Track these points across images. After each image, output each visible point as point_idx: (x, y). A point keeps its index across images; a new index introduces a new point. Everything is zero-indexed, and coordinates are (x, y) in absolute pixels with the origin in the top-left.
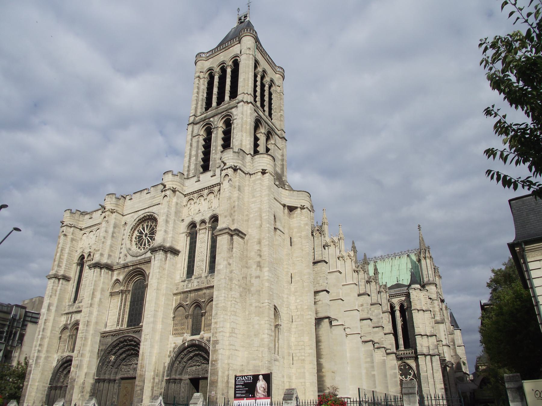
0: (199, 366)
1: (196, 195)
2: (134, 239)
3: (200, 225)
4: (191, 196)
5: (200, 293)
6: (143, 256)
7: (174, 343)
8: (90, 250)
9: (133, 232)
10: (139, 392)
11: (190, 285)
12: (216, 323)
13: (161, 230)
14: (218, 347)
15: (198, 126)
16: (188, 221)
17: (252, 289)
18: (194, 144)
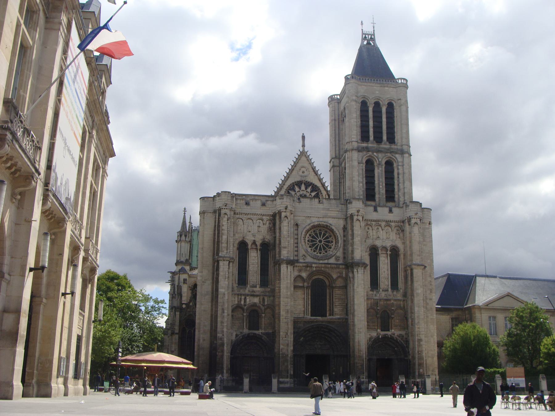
1: (374, 223)
2: (306, 241)
3: (381, 250)
4: (369, 222)
5: (388, 302)
6: (326, 261)
8: (253, 239)
10: (360, 367)
11: (378, 295)
12: (419, 328)
13: (358, 249)
14: (421, 343)
15: (361, 153)
16: (370, 242)
17: (428, 307)
18: (361, 172)
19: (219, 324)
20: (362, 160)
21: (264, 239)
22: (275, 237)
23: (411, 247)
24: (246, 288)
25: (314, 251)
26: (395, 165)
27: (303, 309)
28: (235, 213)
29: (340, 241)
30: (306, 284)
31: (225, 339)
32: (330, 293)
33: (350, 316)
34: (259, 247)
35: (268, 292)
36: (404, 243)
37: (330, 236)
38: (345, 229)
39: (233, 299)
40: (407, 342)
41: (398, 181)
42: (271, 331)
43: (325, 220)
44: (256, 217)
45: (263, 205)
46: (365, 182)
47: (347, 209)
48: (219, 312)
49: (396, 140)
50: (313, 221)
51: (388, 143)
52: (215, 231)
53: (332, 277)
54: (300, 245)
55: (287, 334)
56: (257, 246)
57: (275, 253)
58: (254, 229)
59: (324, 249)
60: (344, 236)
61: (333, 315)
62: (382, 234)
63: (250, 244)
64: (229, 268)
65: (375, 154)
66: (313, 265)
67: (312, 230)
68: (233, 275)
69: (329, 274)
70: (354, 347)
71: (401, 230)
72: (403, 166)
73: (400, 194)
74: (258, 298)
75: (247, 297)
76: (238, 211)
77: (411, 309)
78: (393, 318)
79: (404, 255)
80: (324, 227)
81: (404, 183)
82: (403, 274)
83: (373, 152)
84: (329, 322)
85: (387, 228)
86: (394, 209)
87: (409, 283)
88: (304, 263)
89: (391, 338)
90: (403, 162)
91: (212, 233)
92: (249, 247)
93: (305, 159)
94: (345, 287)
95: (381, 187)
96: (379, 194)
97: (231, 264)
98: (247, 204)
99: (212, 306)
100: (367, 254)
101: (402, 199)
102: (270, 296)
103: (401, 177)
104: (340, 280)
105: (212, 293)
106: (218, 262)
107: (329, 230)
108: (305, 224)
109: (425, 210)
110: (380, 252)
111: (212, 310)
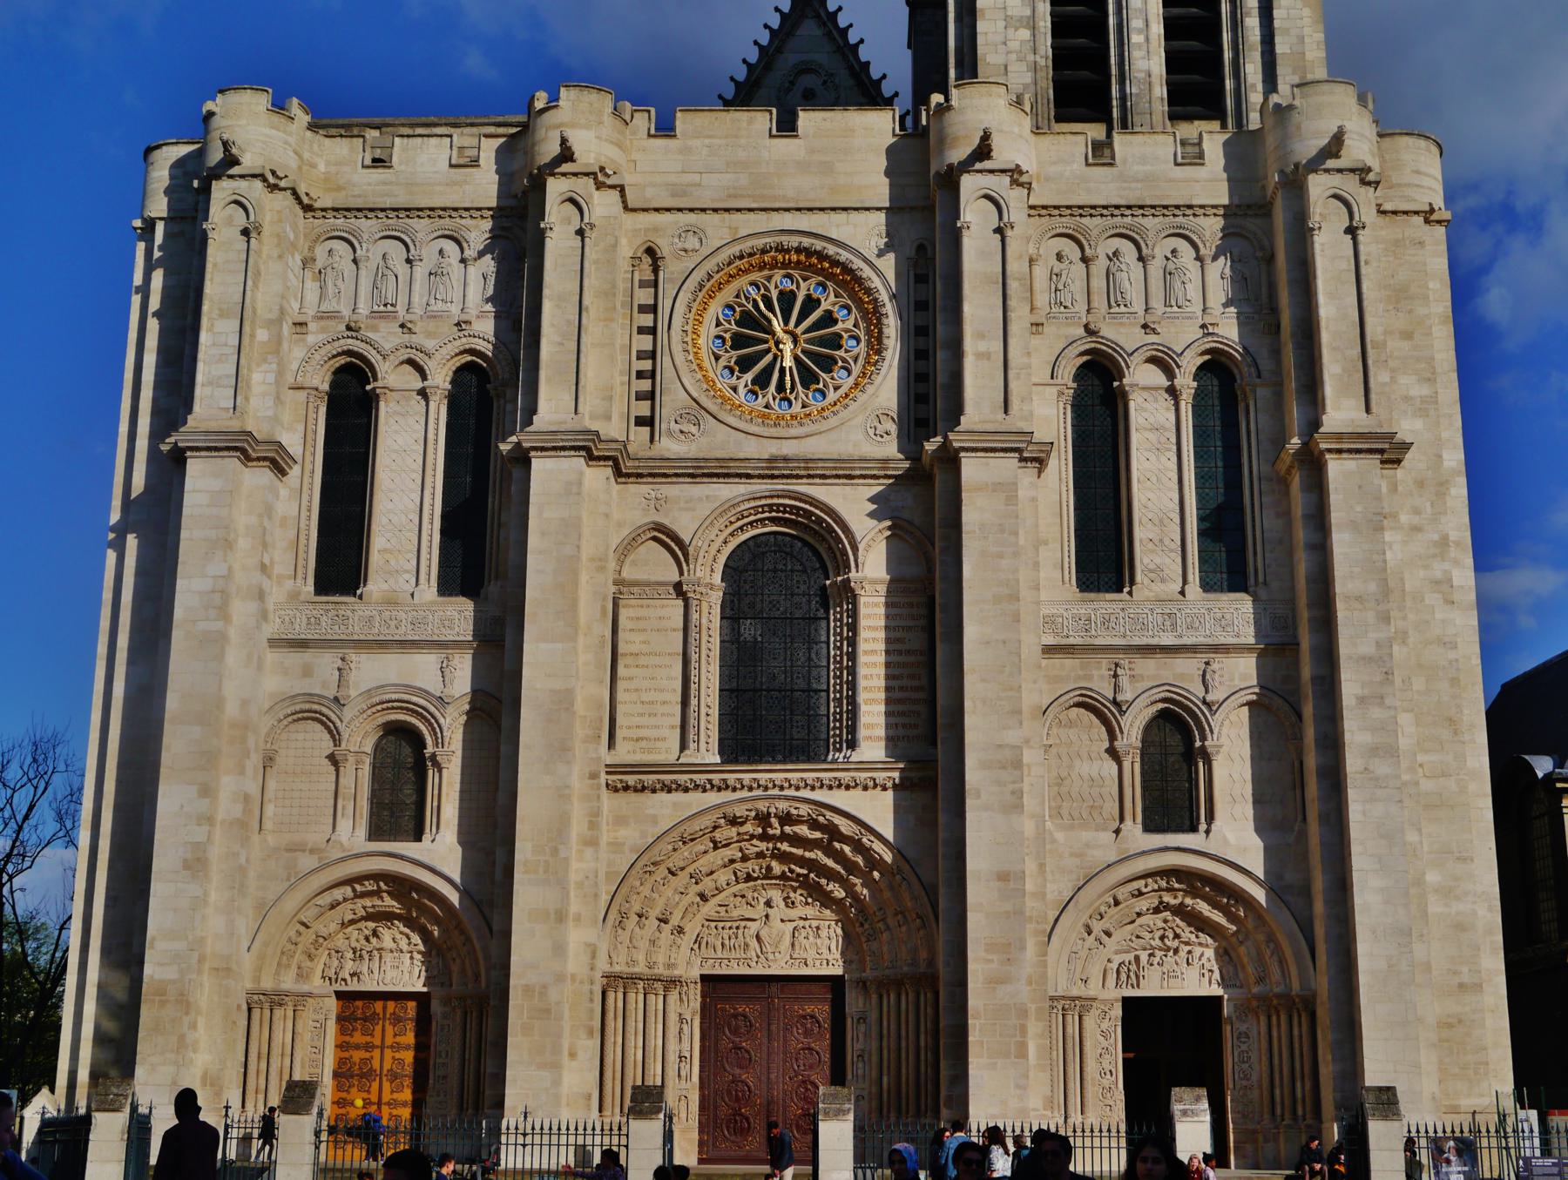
46: (1045, 24)
54: (665, 362)
59: (808, 379)
67: (742, 282)
93: (818, 32)
95: (1136, 38)
101: (1255, 97)
106: (178, 458)
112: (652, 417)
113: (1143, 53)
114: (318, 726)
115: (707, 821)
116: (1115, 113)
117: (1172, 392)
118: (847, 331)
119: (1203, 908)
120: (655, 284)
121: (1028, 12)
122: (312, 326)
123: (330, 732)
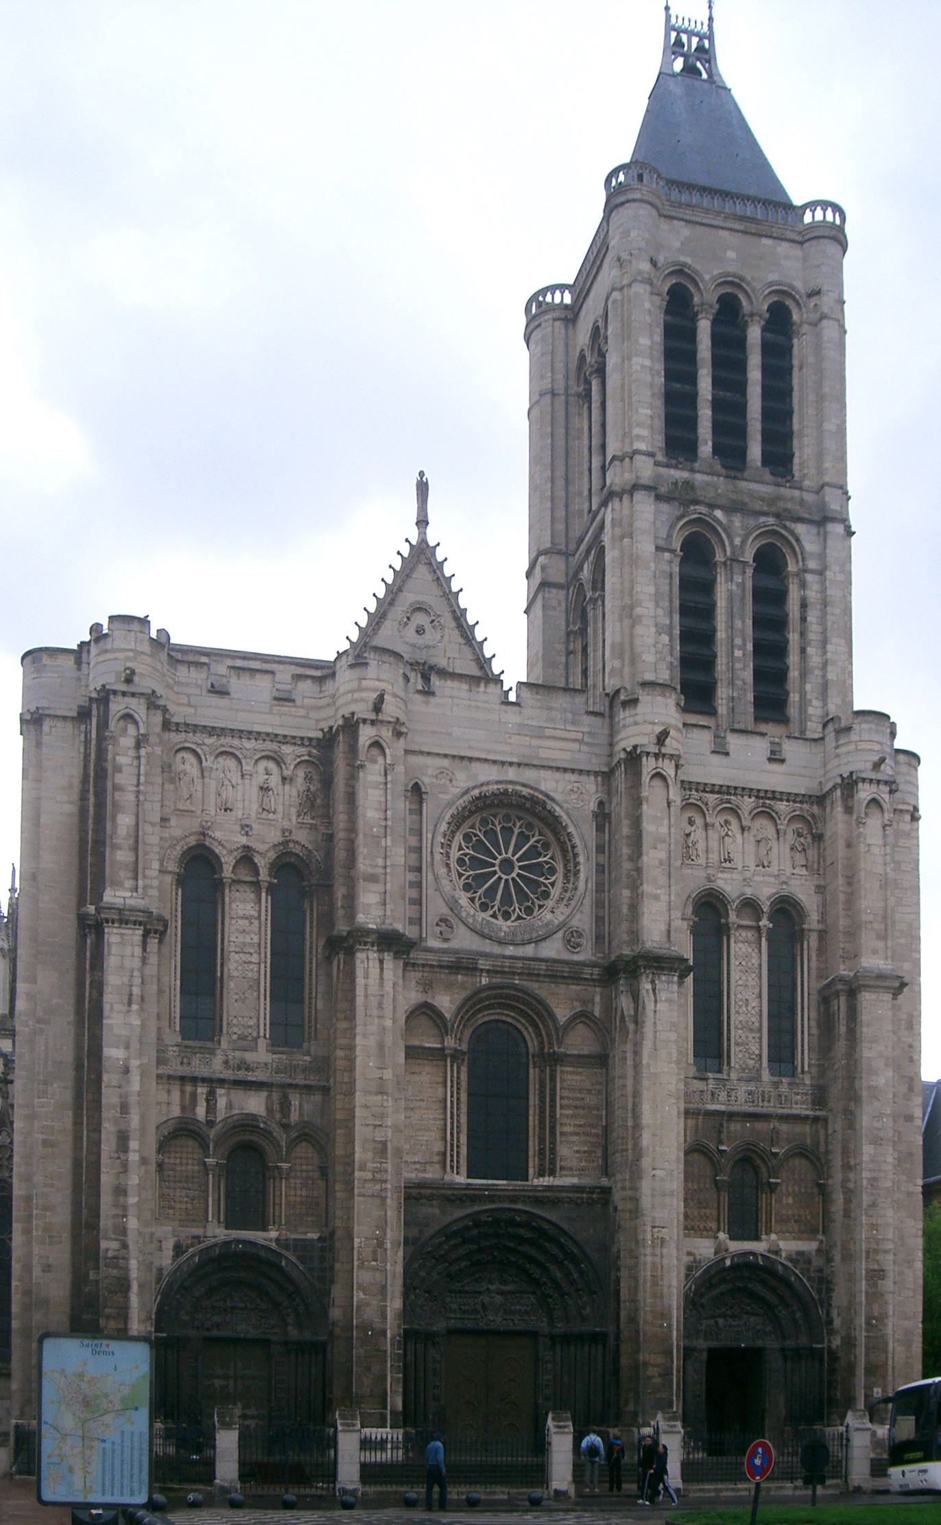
0: (733, 1316)
1: (712, 798)
3: (739, 911)
5: (761, 1126)
6: (529, 950)
7: (689, 1254)
8: (244, 840)
9: (453, 832)
11: (723, 1096)
15: (665, 507)
19: (106, 1199)
20: (669, 536)
21: (285, 843)
22: (330, 838)
23: (850, 903)
24: (212, 1052)
25: (484, 907)
26: (791, 567)
27: (438, 1146)
28: (166, 725)
29: (582, 868)
30: (450, 1042)
31: (133, 1264)
32: (542, 1083)
33: (621, 1177)
34: (264, 875)
35: (304, 1070)
36: (820, 889)
37: (546, 846)
38: (602, 817)
39: (163, 1097)
40: (825, 1283)
41: (803, 634)
42: (313, 1236)
43: (529, 775)
44: (249, 744)
45: (283, 699)
47: (611, 735)
48: (108, 1146)
49: (796, 468)
50: (482, 778)
51: (767, 476)
52: (83, 798)
53: (552, 1016)
54: (427, 877)
55: (381, 1244)
56: (255, 870)
57: (332, 905)
58: (246, 798)
60: (600, 849)
61: (552, 1173)
62: (741, 847)
63: (228, 863)
64: (144, 960)
65: (718, 513)
66: (483, 964)
67: (476, 819)
68: (160, 992)
69: (541, 1002)
70: (634, 1301)
71: (813, 833)
72: (821, 573)
73: (808, 687)
74: (265, 1094)
75: (220, 1091)
76: (180, 713)
77: (846, 1152)
78: (772, 1188)
79: (822, 935)
80: (521, 807)
81: (824, 642)
82: (814, 1014)
83: (712, 506)
84: (538, 1201)
85: (763, 822)
86: (791, 749)
87: (841, 1046)
88: (444, 951)
89: (764, 1269)
90: (822, 557)
91: (72, 809)
92: (227, 872)
94: (602, 1060)
95: (738, 653)
96: (731, 682)
97: (153, 943)
98: (219, 691)
99: (77, 1122)
100: (685, 925)
101: (814, 710)
102: (308, 1089)
103: (812, 617)
104: (581, 1031)
105: (79, 1067)
107: (541, 819)
108: (452, 789)
109: (901, 758)
110: (733, 917)
111: (77, 1138)
112: (421, 919)
113: (741, 666)
114: (191, 1143)
115: (461, 1224)
116: (722, 709)
117: (758, 929)
118: (547, 863)
119: (758, 1288)
120: (421, 814)
121: (668, 622)
122: (173, 822)
123: (201, 1146)
